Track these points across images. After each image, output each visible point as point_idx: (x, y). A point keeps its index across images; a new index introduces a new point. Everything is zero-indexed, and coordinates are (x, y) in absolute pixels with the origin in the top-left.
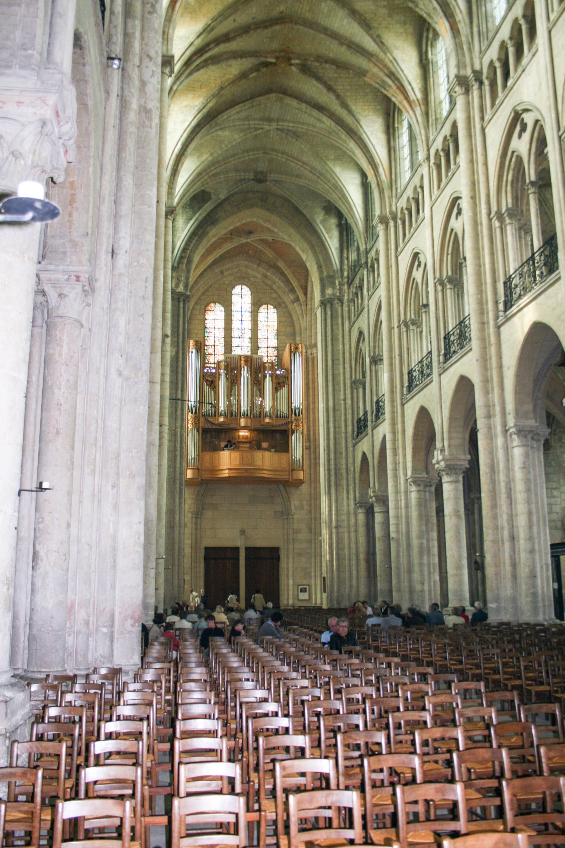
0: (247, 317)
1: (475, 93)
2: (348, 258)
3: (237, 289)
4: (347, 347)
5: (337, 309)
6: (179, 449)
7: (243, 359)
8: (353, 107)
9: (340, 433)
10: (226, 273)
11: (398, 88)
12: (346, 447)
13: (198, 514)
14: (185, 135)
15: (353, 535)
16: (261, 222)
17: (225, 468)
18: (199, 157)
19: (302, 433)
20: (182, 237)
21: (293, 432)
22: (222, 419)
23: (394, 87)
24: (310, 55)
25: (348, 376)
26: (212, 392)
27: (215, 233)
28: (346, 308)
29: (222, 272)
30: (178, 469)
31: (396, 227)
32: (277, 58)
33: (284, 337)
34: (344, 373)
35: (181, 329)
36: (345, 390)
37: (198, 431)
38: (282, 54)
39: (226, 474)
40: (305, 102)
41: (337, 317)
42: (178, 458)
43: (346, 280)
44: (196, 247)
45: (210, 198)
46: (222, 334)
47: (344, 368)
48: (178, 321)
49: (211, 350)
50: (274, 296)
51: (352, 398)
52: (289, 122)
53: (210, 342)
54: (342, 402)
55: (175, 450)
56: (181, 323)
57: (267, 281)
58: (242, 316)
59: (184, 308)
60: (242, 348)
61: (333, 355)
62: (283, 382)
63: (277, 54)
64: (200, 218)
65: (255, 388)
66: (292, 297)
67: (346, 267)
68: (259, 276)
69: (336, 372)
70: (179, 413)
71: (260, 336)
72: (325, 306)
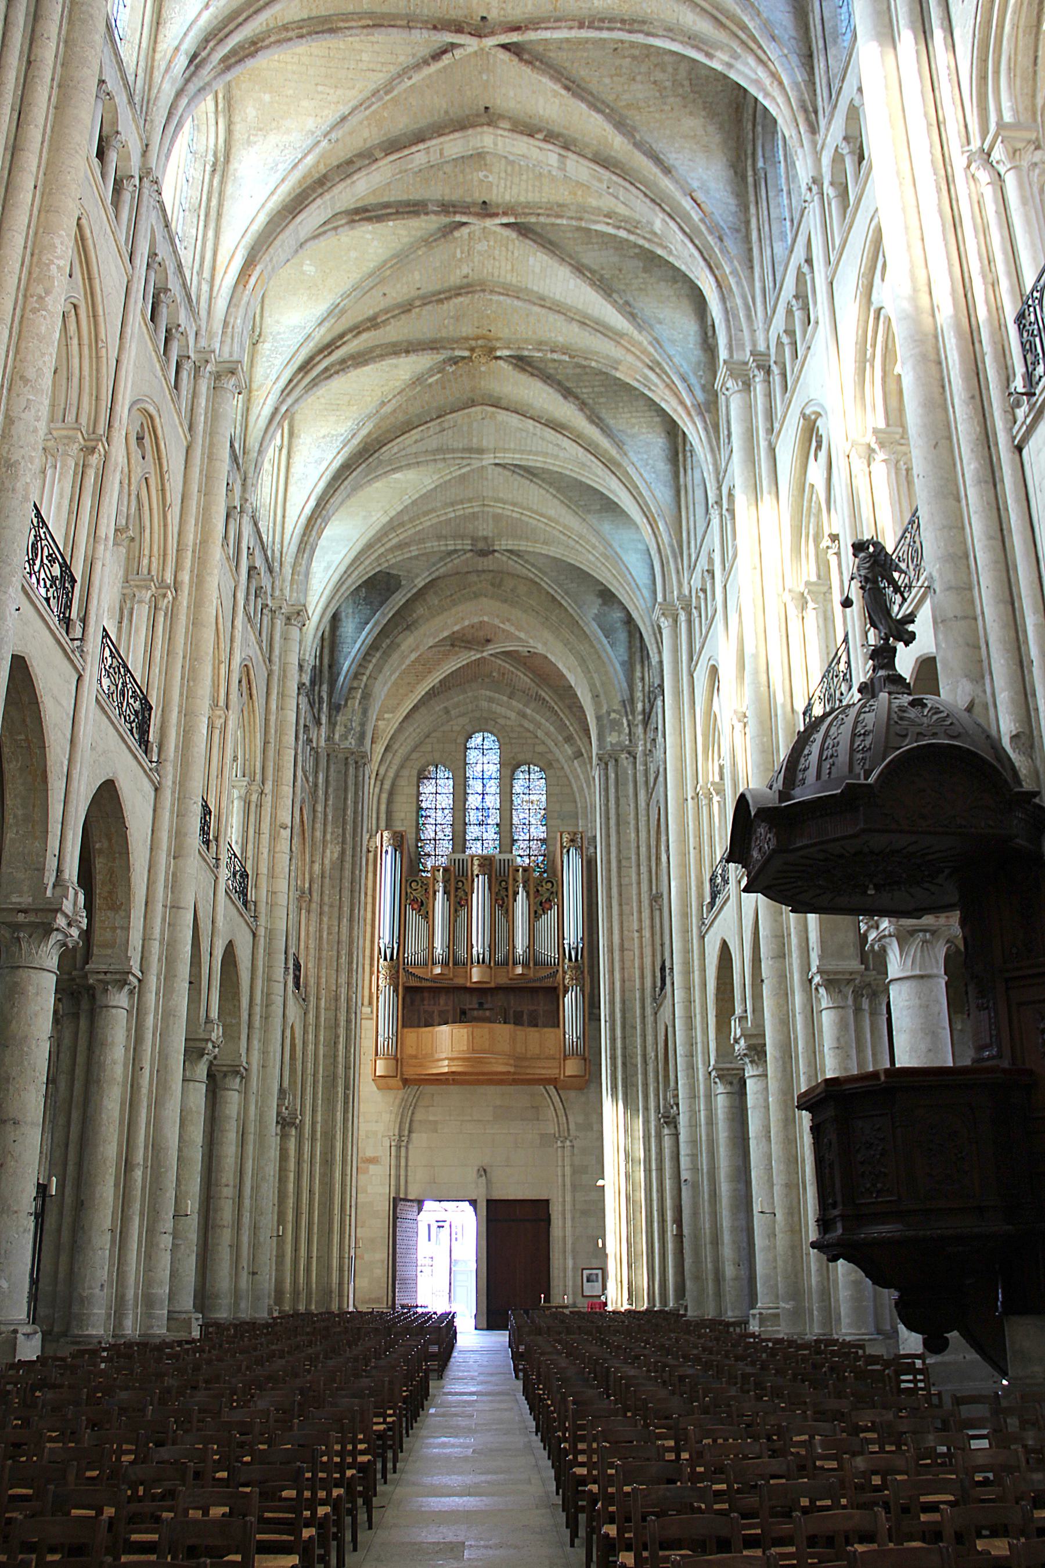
0: (493, 787)
1: (759, 388)
2: (643, 679)
3: (477, 740)
4: (643, 835)
5: (626, 769)
6: (342, 1023)
7: (476, 862)
11: (667, 386)
12: (643, 1017)
13: (402, 1141)
14: (322, 485)
16: (496, 622)
17: (443, 1056)
19: (582, 991)
20: (353, 654)
21: (566, 991)
22: (438, 970)
23: (661, 386)
24: (526, 341)
25: (645, 887)
26: (422, 922)
27: (414, 645)
29: (447, 711)
30: (341, 1059)
32: (472, 350)
34: (639, 883)
35: (350, 812)
36: (640, 912)
37: (396, 990)
38: (480, 342)
41: (626, 784)
43: (640, 717)
44: (379, 668)
45: (399, 586)
46: (449, 818)
47: (639, 874)
48: (346, 799)
51: (652, 927)
52: (514, 451)
53: (429, 833)
55: (337, 1025)
57: (526, 724)
58: (484, 786)
59: (356, 777)
60: (483, 840)
61: (619, 851)
63: (473, 343)
65: (498, 913)
66: (569, 751)
67: (639, 695)
68: (513, 715)
70: (343, 959)
71: (515, 821)
72: (606, 764)
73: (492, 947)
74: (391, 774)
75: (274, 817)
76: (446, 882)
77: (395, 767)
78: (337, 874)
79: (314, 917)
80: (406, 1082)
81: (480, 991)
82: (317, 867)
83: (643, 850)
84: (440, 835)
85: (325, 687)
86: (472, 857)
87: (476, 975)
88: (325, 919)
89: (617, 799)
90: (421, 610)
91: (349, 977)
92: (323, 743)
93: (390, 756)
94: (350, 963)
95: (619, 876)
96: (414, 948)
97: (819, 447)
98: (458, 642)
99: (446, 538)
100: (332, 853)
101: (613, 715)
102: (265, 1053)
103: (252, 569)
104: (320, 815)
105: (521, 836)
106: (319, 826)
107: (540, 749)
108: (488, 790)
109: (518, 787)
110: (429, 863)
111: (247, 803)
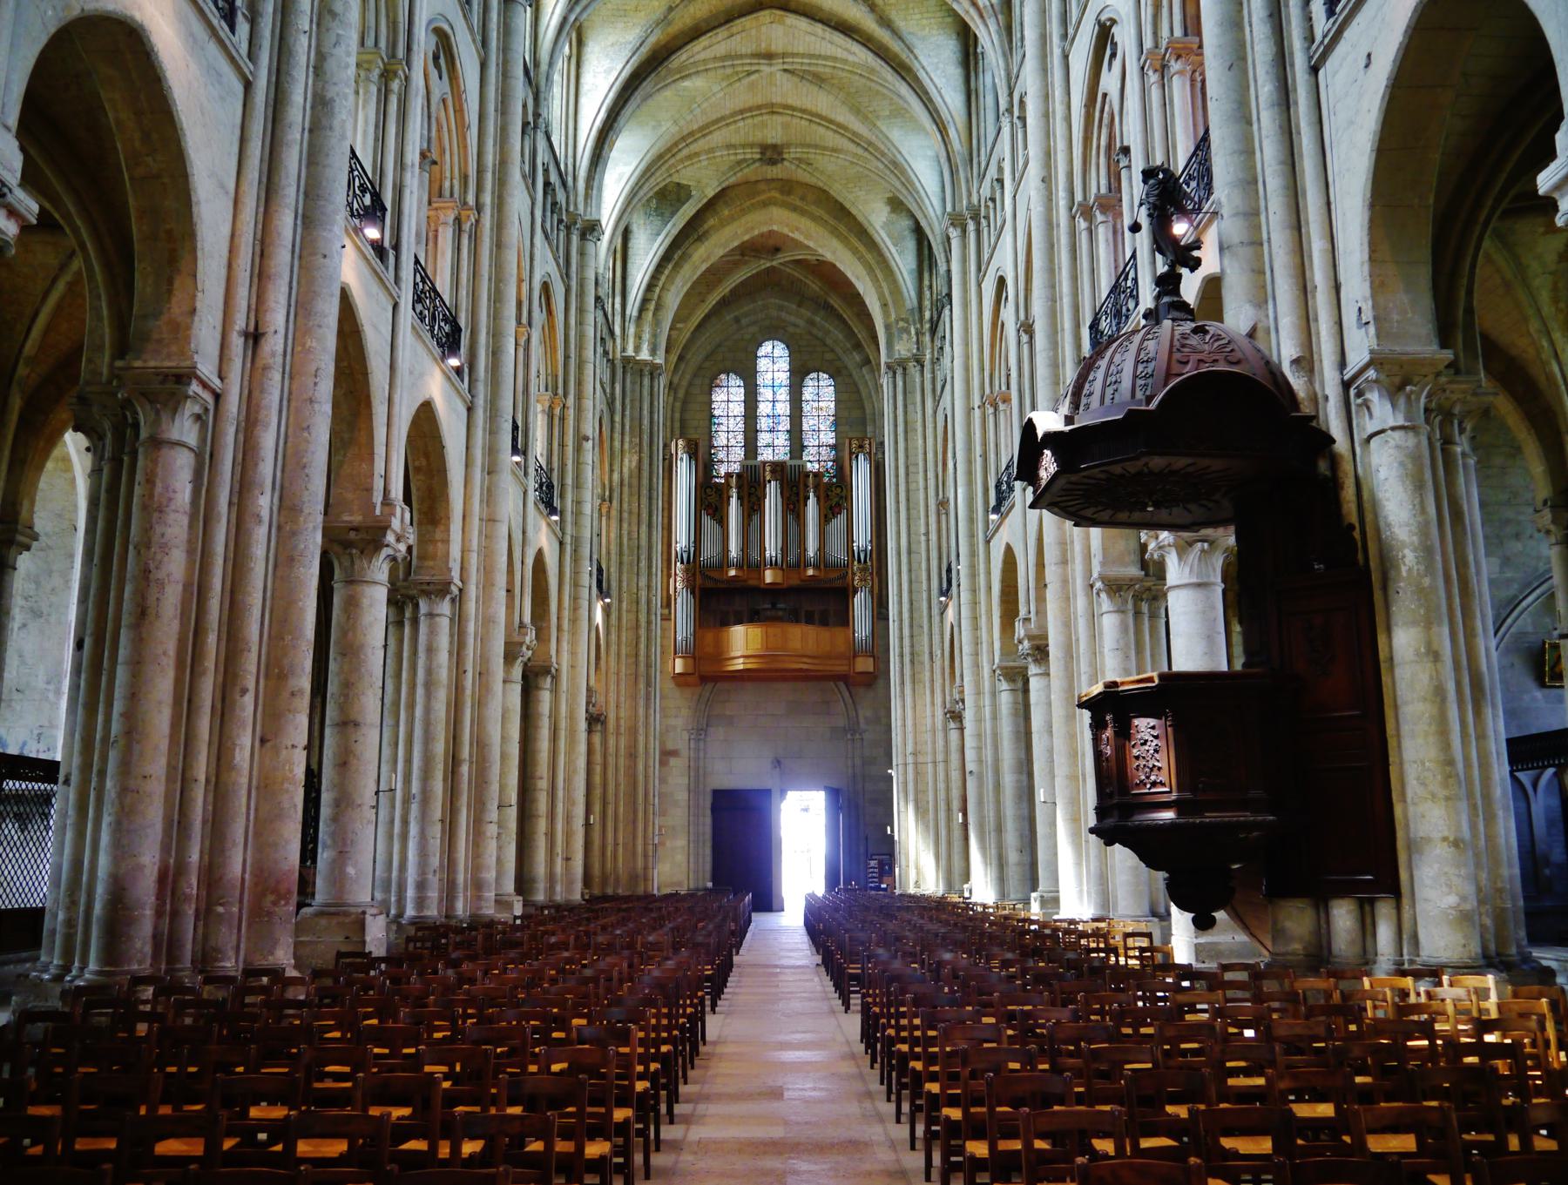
0: (783, 394)
2: (931, 287)
3: (766, 348)
8: (900, 23)
9: (920, 592)
10: (744, 322)
12: (930, 617)
13: (700, 731)
14: (611, 95)
15: (941, 767)
16: (786, 231)
17: (739, 654)
18: (654, 128)
19: (871, 592)
21: (855, 591)
22: (732, 573)
26: (717, 526)
27: (705, 255)
28: (928, 376)
29: (737, 320)
30: (642, 658)
31: (978, 232)
33: (847, 428)
35: (646, 422)
37: (693, 593)
39: (739, 665)
40: (821, 21)
41: (913, 392)
42: (643, 639)
43: (927, 326)
44: (670, 279)
45: (689, 196)
46: (741, 425)
47: (926, 480)
49: (722, 455)
50: (829, 356)
53: (721, 440)
54: (923, 538)
55: (637, 626)
56: (646, 412)
57: (815, 331)
59: (652, 387)
60: (773, 447)
61: (907, 457)
62: (838, 505)
64: (675, 232)
66: (858, 358)
67: (927, 303)
68: (801, 323)
69: (912, 486)
70: (643, 564)
71: (805, 427)
73: (784, 550)
74: (685, 383)
75: (577, 429)
76: (739, 487)
77: (688, 377)
78: (635, 482)
79: (614, 524)
80: (704, 679)
81: (773, 591)
82: (616, 476)
83: (930, 456)
84: (733, 442)
85: (618, 300)
86: (764, 463)
87: (769, 576)
88: (625, 525)
89: (905, 406)
90: (711, 222)
91: (649, 580)
92: (618, 355)
93: (682, 366)
94: (650, 567)
95: (907, 482)
96: (709, 552)
97: (1113, 55)
98: (749, 250)
99: (734, 146)
100: (630, 462)
101: (901, 324)
102: (573, 653)
103: (547, 184)
104: (618, 426)
105: (810, 441)
106: (617, 436)
107: (829, 356)
108: (778, 397)
109: (808, 394)
110: (723, 470)
111: (551, 417)
